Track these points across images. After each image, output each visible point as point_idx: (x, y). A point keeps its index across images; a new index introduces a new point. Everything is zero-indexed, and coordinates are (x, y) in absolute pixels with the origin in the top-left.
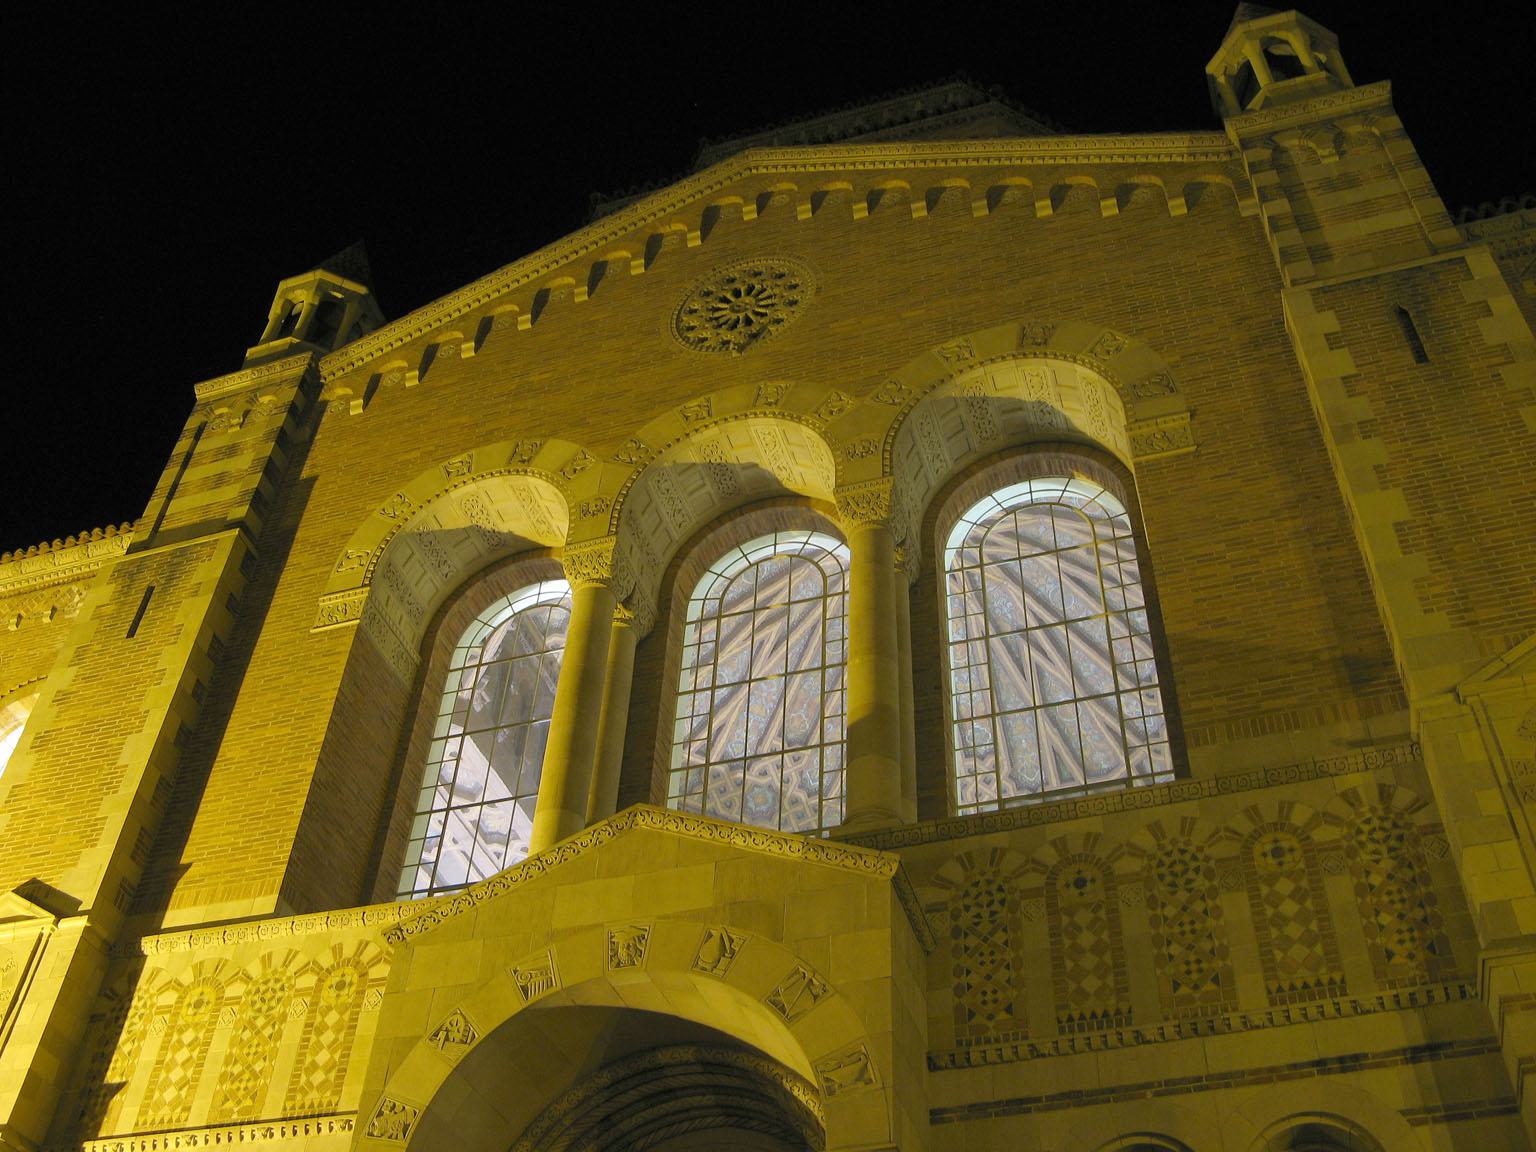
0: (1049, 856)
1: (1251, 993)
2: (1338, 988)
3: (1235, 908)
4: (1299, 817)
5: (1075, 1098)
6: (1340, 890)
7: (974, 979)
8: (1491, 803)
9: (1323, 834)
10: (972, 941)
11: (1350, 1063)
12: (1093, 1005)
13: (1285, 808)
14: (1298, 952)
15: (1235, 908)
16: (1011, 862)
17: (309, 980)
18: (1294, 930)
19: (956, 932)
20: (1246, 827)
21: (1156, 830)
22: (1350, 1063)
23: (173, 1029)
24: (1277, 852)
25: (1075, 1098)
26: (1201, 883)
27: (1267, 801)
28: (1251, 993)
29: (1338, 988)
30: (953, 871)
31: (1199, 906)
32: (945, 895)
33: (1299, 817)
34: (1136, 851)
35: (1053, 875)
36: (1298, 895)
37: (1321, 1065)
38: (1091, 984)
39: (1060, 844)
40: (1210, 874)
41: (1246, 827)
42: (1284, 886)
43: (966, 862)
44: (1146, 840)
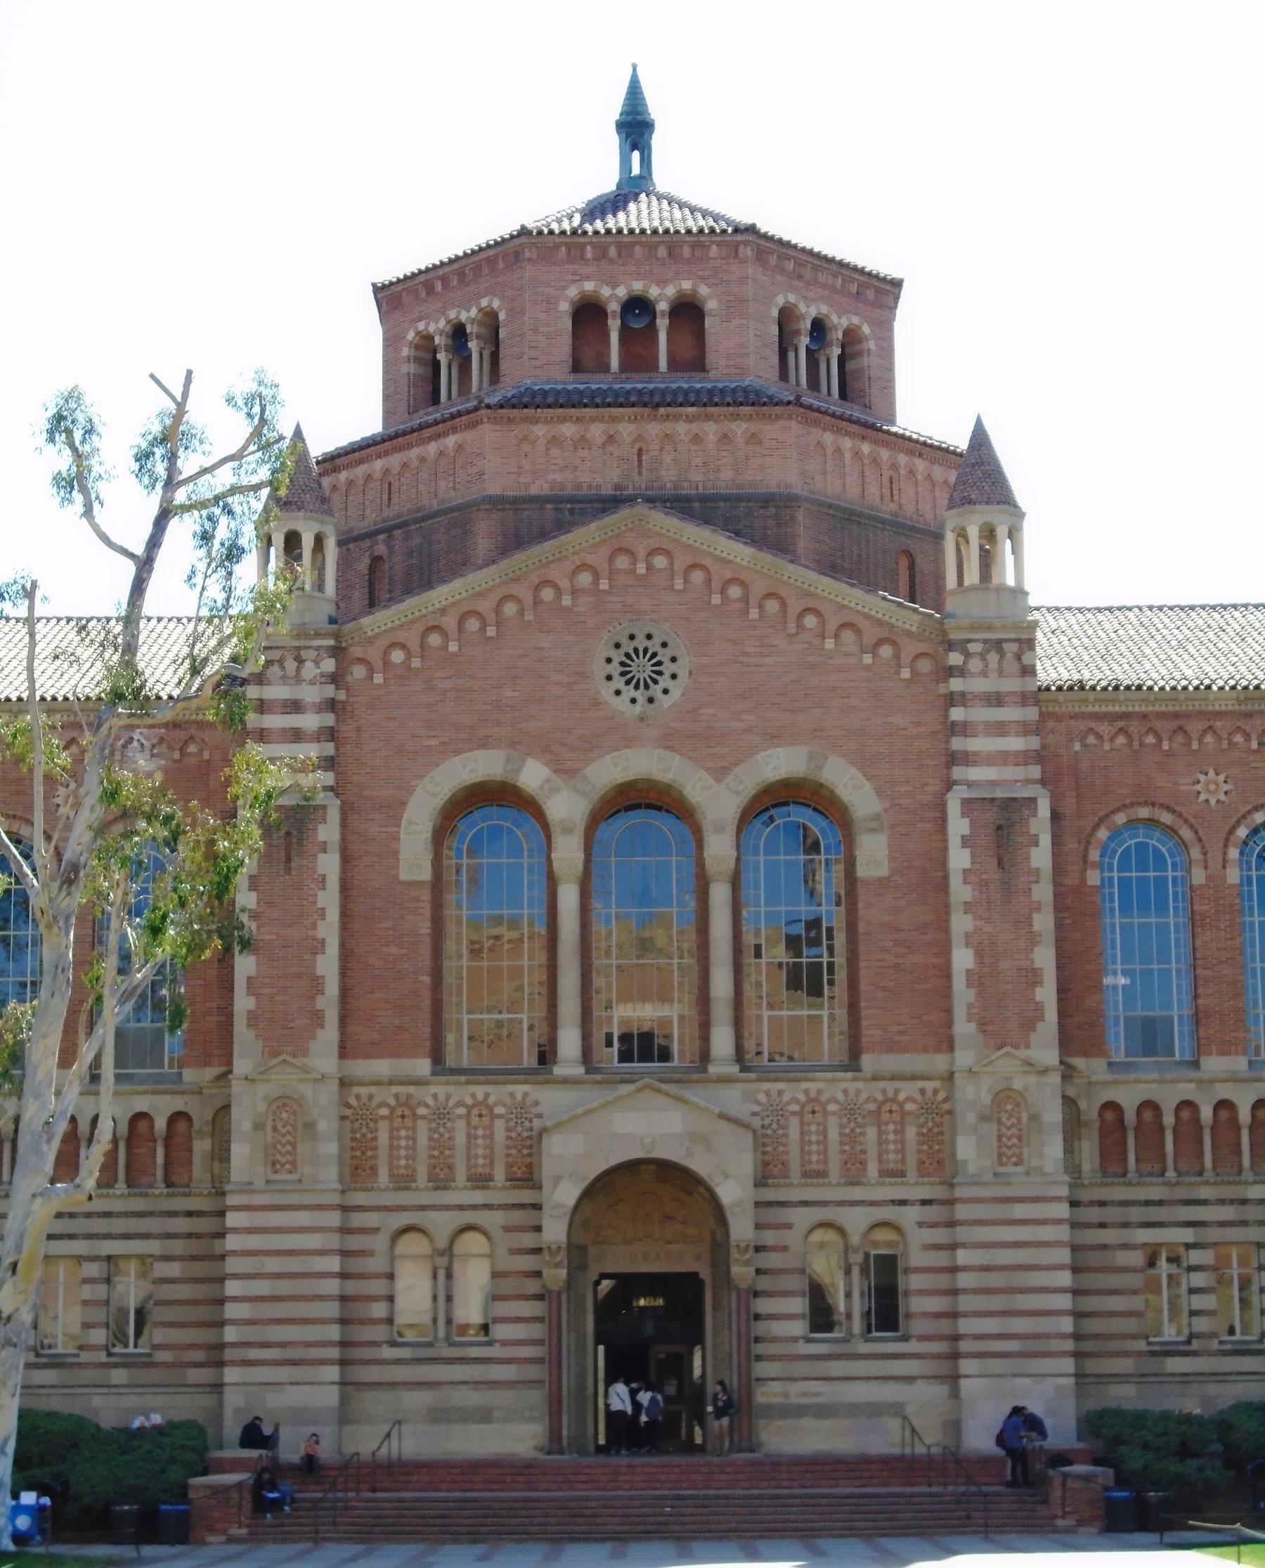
0: (802, 1098)
1: (873, 1170)
2: (902, 1174)
3: (872, 1132)
4: (902, 1097)
5: (805, 1203)
6: (911, 1132)
7: (769, 1149)
8: (971, 1118)
9: (910, 1107)
10: (769, 1132)
11: (902, 1203)
12: (814, 1166)
13: (897, 1092)
14: (892, 1156)
15: (872, 1132)
16: (786, 1097)
17: (462, 1111)
18: (891, 1147)
19: (763, 1127)
20: (880, 1097)
21: (845, 1092)
22: (902, 1203)
23: (392, 1129)
24: (891, 1112)
25: (805, 1203)
26: (860, 1120)
27: (890, 1086)
28: (873, 1170)
29: (902, 1174)
30: (762, 1098)
31: (858, 1130)
32: (756, 1108)
33: (902, 1097)
34: (836, 1101)
35: (803, 1107)
36: (895, 1132)
37: (893, 1202)
38: (814, 1158)
39: (806, 1092)
40: (864, 1117)
41: (880, 1097)
42: (891, 1127)
43: (768, 1093)
44: (841, 1097)
